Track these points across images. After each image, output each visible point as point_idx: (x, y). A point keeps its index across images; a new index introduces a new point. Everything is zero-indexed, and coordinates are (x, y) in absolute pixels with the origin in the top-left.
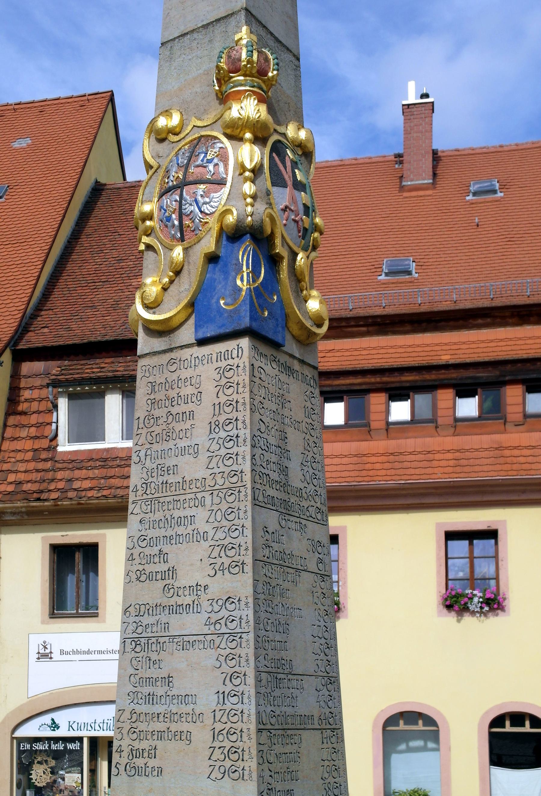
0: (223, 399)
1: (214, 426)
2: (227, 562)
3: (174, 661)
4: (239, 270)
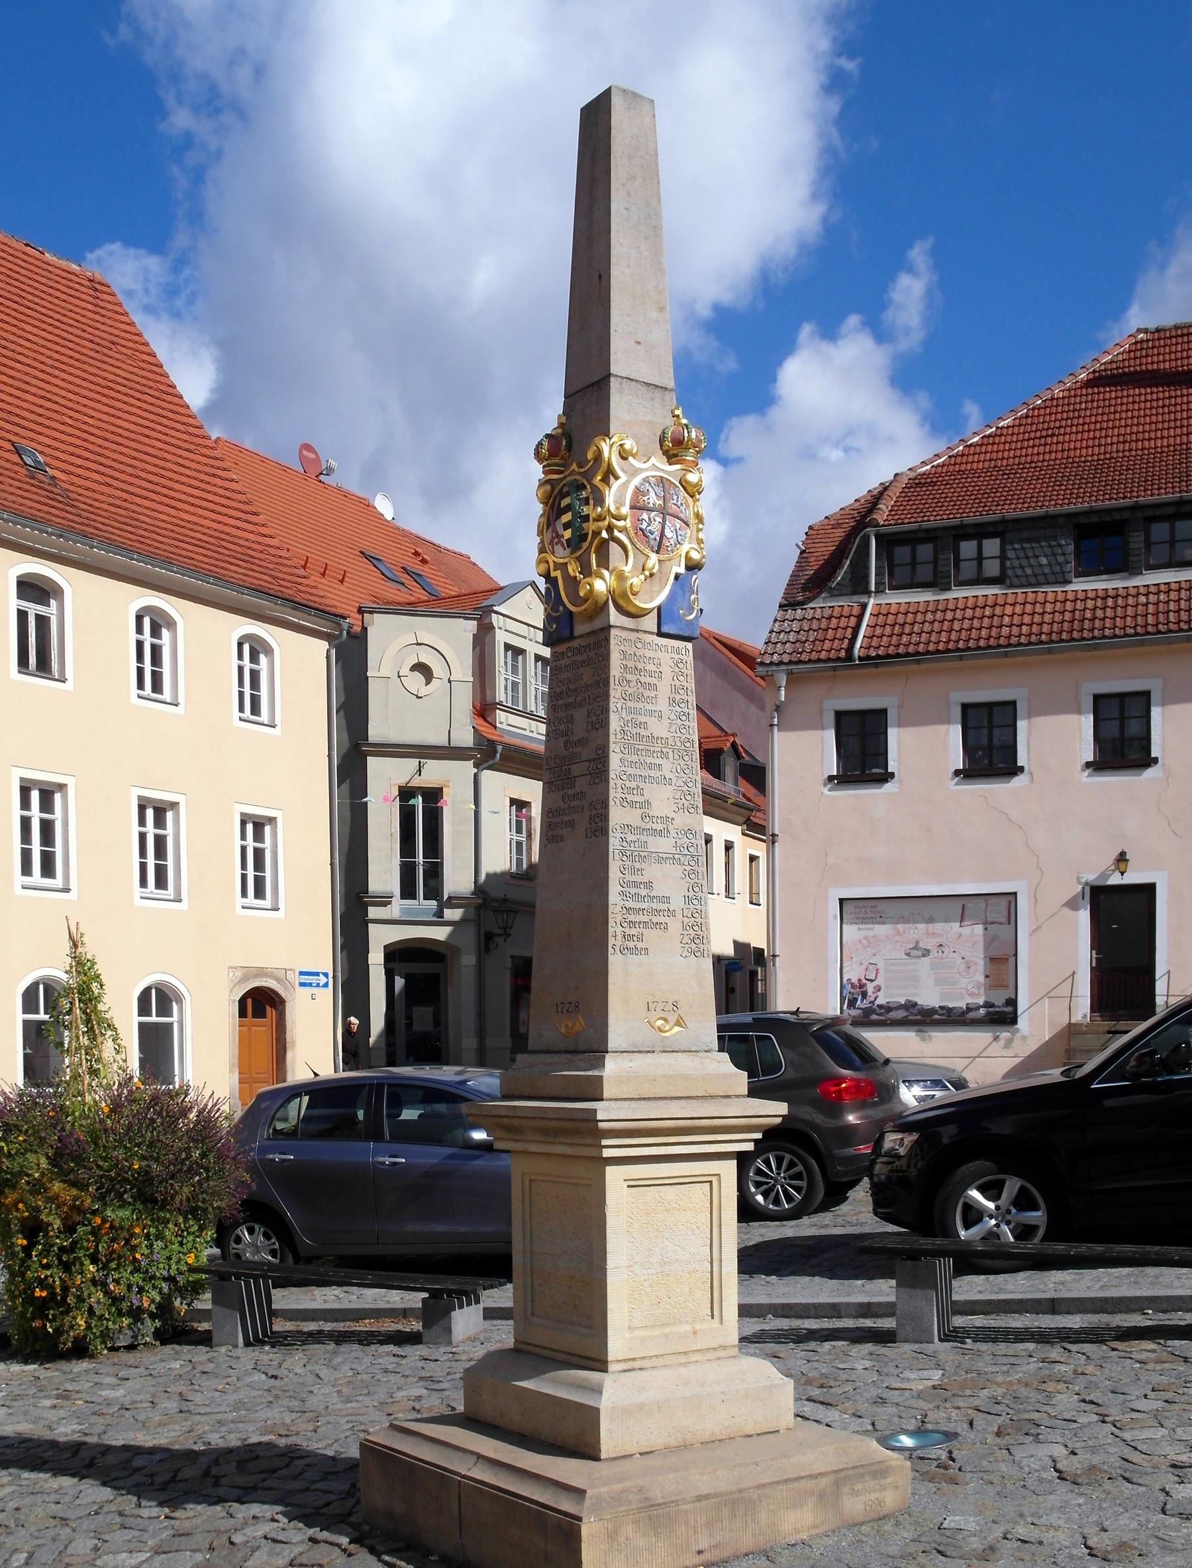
3: (652, 872)
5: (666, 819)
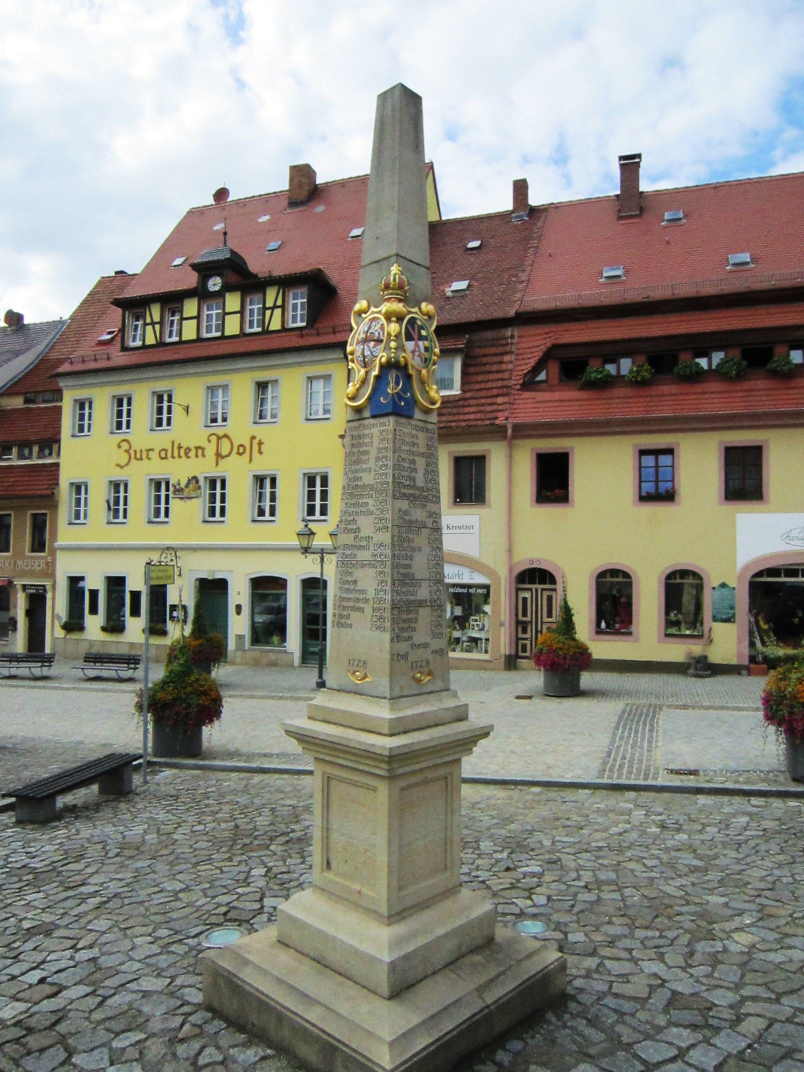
0: (381, 446)
1: (378, 459)
2: (381, 526)
3: (359, 574)
4: (389, 383)
5: (369, 538)
